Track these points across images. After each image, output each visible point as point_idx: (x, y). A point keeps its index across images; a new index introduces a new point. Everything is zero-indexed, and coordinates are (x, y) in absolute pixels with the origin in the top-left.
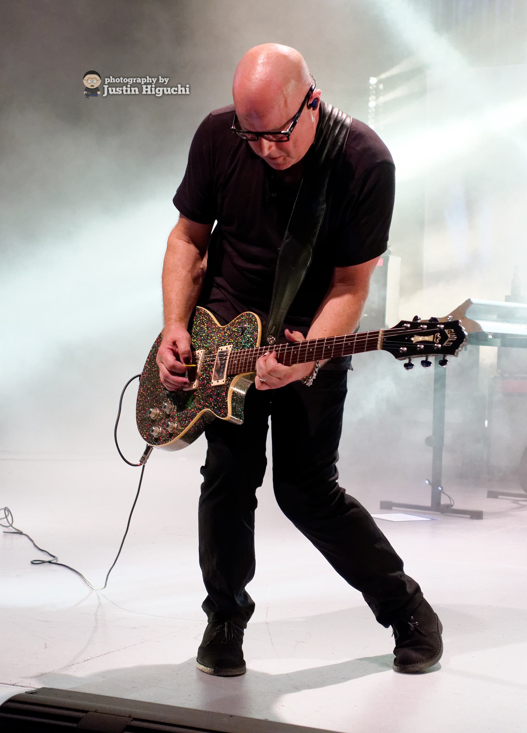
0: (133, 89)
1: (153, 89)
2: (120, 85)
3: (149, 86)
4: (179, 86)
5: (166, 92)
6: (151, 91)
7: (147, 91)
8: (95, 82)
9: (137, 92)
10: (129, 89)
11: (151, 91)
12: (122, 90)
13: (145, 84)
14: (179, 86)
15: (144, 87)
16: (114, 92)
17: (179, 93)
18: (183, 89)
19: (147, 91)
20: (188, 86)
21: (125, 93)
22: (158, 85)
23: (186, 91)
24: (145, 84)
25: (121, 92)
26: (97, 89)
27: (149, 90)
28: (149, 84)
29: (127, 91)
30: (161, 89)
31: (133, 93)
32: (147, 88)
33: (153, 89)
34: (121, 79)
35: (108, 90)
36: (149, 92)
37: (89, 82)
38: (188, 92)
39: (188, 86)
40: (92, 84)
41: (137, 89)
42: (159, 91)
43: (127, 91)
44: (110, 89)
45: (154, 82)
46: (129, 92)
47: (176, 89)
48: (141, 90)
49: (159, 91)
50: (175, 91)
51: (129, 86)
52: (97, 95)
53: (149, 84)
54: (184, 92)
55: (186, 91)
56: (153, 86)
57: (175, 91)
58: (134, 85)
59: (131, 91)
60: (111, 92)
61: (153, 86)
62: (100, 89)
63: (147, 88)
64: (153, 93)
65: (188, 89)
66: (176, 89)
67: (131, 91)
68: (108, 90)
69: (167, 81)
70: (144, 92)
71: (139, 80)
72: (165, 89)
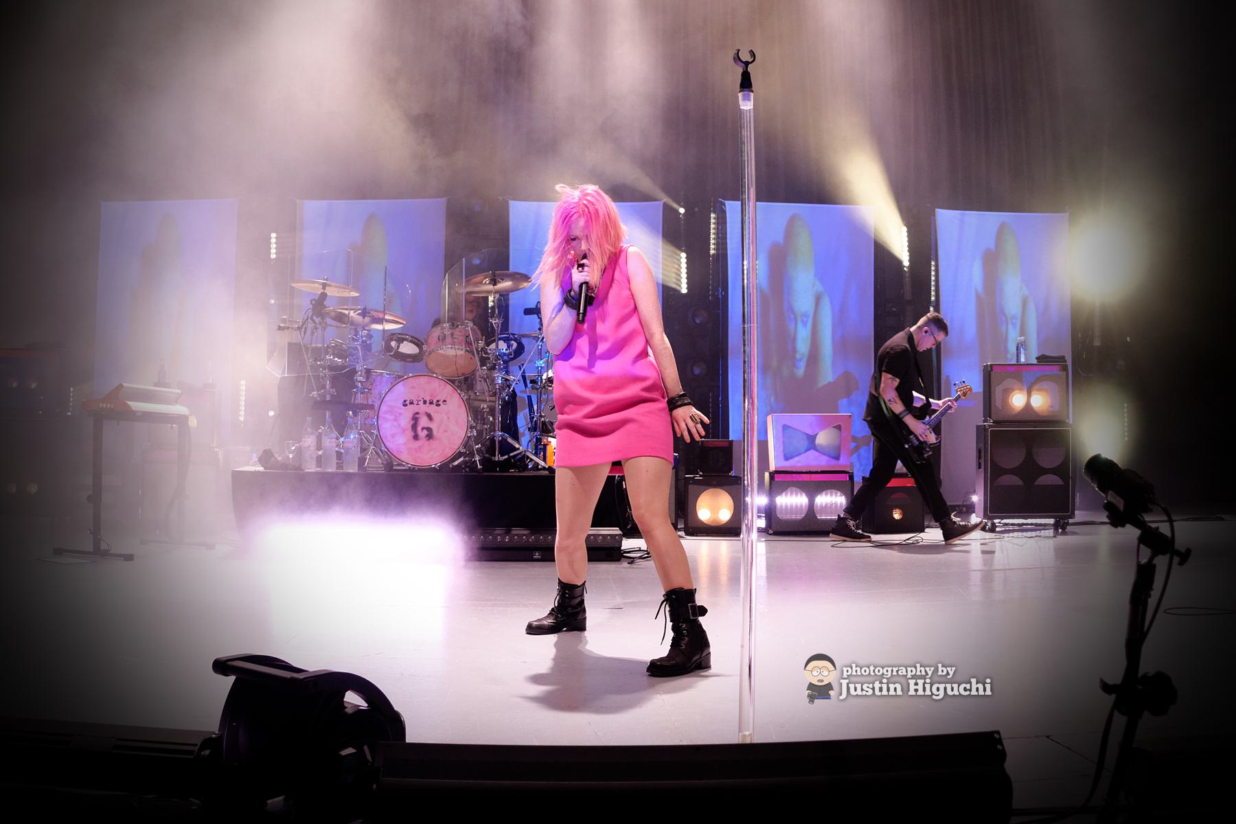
0: (892, 686)
1: (928, 686)
2: (870, 679)
3: (921, 682)
4: (974, 681)
5: (949, 692)
6: (924, 690)
7: (916, 690)
8: (825, 673)
9: (899, 692)
10: (884, 687)
11: (924, 690)
12: (873, 689)
13: (913, 677)
14: (974, 681)
15: (912, 682)
16: (859, 692)
17: (974, 692)
18: (980, 686)
19: (916, 690)
20: (988, 681)
21: (877, 693)
22: (935, 679)
23: (985, 690)
24: (913, 677)
25: (871, 692)
26: (829, 687)
27: (920, 687)
28: (924, 677)
29: (881, 690)
30: (942, 686)
31: (892, 692)
32: (916, 684)
33: (928, 686)
34: (872, 668)
35: (848, 689)
36: (920, 692)
37: (815, 673)
38: (988, 692)
39: (988, 681)
40: (820, 677)
41: (898, 686)
42: (938, 689)
43: (881, 690)
44: (852, 686)
45: (930, 673)
46: (885, 692)
47: (968, 686)
48: (906, 689)
49: (938, 689)
50: (965, 689)
51: (885, 681)
52: (828, 697)
53: (924, 677)
54: (981, 692)
55: (985, 690)
56: (928, 681)
57: (965, 689)
58: (894, 679)
59: (888, 690)
60: (852, 692)
61: (928, 681)
62: (835, 686)
63: (916, 684)
64: (928, 692)
65: (988, 687)
66: (968, 686)
67: (888, 690)
68: (848, 689)
69: (951, 673)
70: (912, 692)
71: (903, 671)
72: (949, 686)
